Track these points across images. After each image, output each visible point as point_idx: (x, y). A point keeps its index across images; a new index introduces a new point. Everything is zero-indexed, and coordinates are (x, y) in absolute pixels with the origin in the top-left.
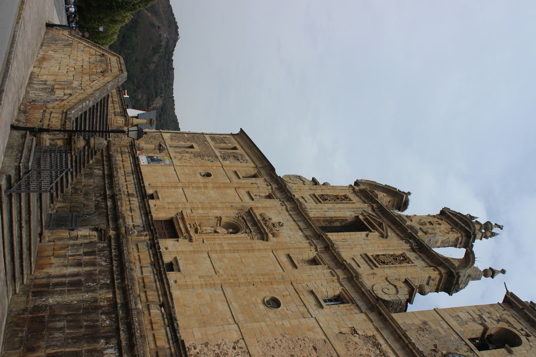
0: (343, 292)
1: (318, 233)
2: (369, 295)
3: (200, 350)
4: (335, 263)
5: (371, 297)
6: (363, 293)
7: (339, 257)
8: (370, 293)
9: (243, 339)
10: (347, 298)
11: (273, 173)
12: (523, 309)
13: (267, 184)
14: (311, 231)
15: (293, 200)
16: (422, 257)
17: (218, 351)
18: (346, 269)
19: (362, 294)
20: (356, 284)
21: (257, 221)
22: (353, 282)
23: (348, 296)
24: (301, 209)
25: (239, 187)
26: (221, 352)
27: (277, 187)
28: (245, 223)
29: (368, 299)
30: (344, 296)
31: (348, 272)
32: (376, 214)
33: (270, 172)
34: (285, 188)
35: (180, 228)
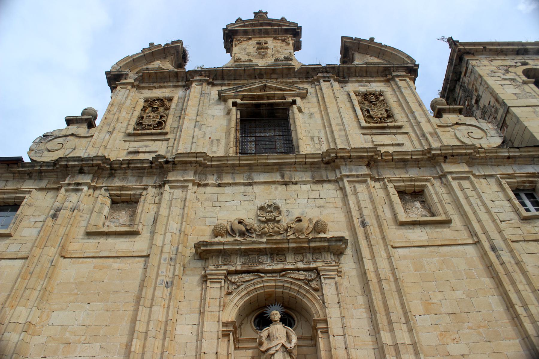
0: (508, 180)
1: (317, 160)
2: (520, 152)
4: (413, 167)
5: (524, 152)
6: (509, 157)
7: (408, 155)
8: (517, 150)
10: (525, 180)
11: (23, 167)
12: (484, 48)
13: (67, 191)
14: (297, 171)
15: (174, 163)
16: (363, 80)
18: (448, 157)
19: (510, 160)
20: (486, 158)
21: (268, 246)
22: (478, 161)
23: (521, 177)
24: (211, 161)
25: (63, 248)
27: (91, 176)
28: (262, 275)
29: (525, 157)
30: (518, 182)
31: (457, 157)
32: (234, 84)
33: (14, 173)
34: (111, 164)
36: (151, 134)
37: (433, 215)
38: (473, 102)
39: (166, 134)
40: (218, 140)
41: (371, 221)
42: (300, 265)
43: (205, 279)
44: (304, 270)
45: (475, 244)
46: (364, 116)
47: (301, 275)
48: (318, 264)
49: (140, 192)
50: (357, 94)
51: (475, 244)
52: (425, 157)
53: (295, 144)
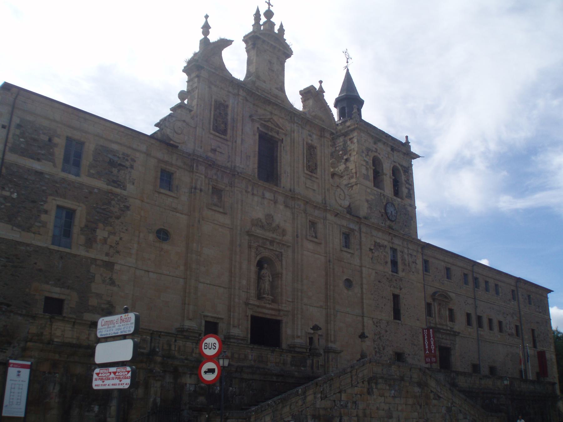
3: (377, 346)
9: (373, 318)
17: (378, 336)
26: (379, 335)
35: (272, 315)
36: (221, 138)
37: (316, 237)
38: (345, 157)
39: (227, 140)
40: (249, 156)
41: (299, 235)
42: (278, 250)
43: (250, 247)
44: (278, 251)
45: (325, 256)
46: (307, 164)
47: (277, 253)
48: (283, 251)
49: (224, 187)
50: (307, 143)
51: (325, 256)
52: (324, 208)
53: (279, 173)
